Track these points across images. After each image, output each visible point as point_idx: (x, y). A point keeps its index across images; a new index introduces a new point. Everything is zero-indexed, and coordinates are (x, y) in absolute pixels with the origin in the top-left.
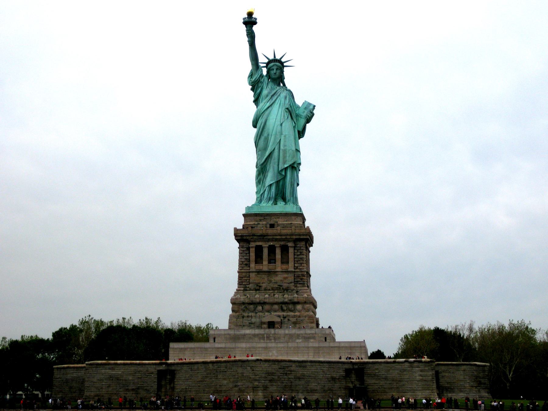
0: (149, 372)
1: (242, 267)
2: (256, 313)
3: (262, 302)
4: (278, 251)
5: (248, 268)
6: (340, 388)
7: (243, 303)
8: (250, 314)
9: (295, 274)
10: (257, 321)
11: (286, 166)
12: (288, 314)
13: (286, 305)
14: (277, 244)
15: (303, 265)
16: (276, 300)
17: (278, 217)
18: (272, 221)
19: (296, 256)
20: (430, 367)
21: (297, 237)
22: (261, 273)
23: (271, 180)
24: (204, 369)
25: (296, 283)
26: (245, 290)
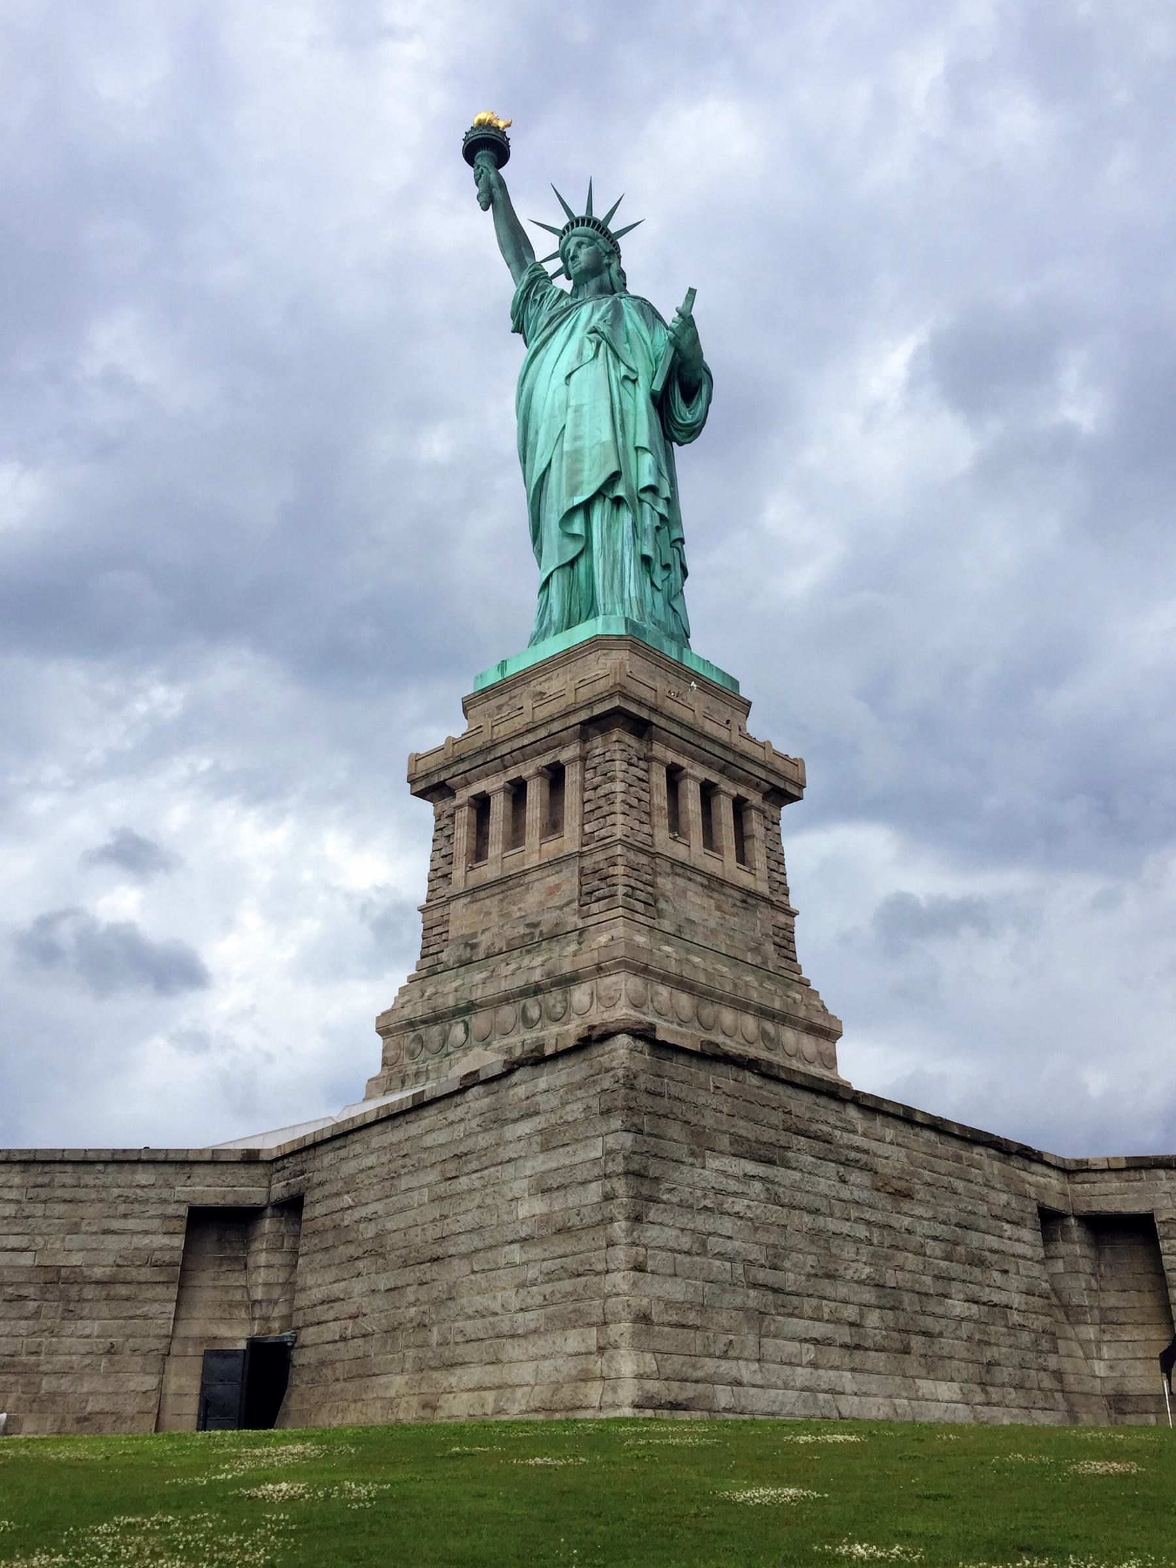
2: (448, 1055)
3: (462, 1004)
4: (535, 793)
6: (111, 1351)
7: (411, 1024)
9: (588, 863)
11: (578, 500)
14: (527, 770)
16: (505, 985)
17: (548, 675)
19: (587, 795)
20: (592, 1092)
21: (584, 716)
22: (483, 894)
25: (587, 899)
26: (432, 972)
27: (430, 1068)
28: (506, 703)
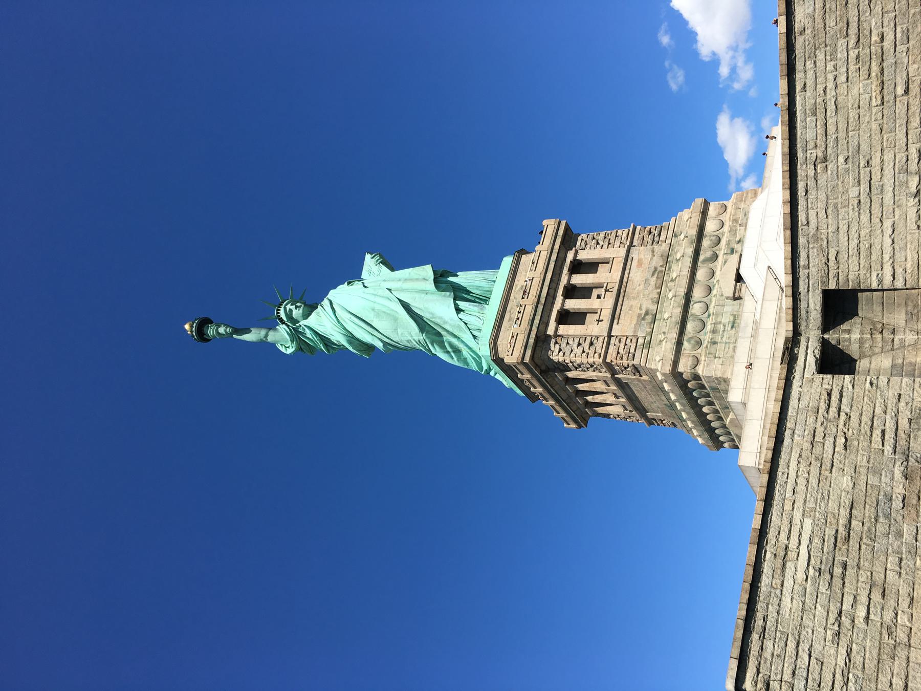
0: (823, 406)
1: (595, 353)
3: (683, 301)
4: (579, 279)
5: (601, 339)
7: (679, 344)
8: (709, 327)
10: (730, 310)
12: (723, 248)
13: (701, 252)
14: (564, 280)
15: (620, 232)
16: (686, 272)
18: (517, 296)
22: (618, 310)
23: (449, 307)
24: (820, 56)
27: (713, 321)
28: (511, 314)
